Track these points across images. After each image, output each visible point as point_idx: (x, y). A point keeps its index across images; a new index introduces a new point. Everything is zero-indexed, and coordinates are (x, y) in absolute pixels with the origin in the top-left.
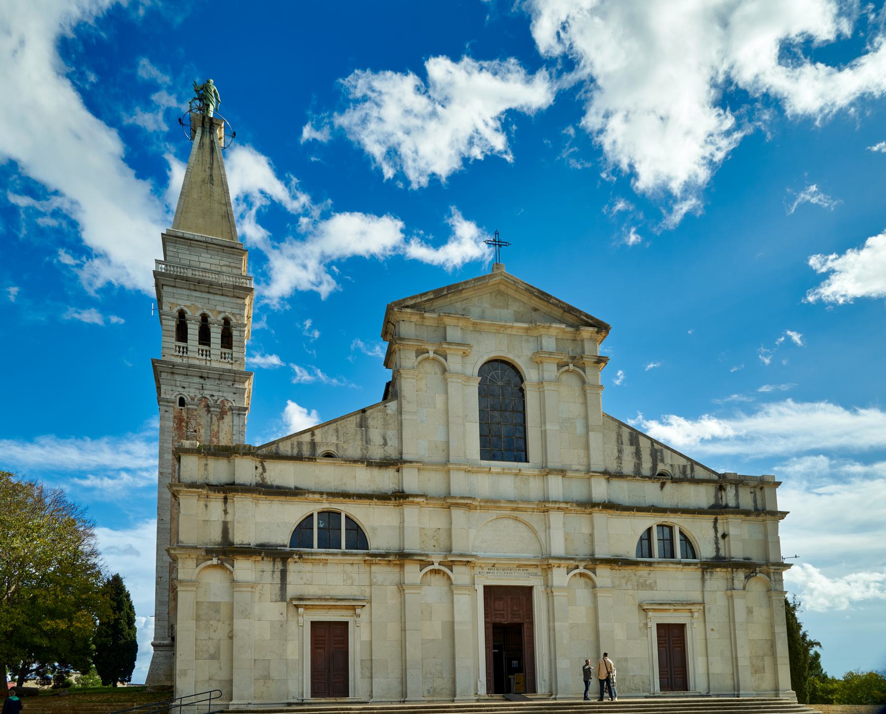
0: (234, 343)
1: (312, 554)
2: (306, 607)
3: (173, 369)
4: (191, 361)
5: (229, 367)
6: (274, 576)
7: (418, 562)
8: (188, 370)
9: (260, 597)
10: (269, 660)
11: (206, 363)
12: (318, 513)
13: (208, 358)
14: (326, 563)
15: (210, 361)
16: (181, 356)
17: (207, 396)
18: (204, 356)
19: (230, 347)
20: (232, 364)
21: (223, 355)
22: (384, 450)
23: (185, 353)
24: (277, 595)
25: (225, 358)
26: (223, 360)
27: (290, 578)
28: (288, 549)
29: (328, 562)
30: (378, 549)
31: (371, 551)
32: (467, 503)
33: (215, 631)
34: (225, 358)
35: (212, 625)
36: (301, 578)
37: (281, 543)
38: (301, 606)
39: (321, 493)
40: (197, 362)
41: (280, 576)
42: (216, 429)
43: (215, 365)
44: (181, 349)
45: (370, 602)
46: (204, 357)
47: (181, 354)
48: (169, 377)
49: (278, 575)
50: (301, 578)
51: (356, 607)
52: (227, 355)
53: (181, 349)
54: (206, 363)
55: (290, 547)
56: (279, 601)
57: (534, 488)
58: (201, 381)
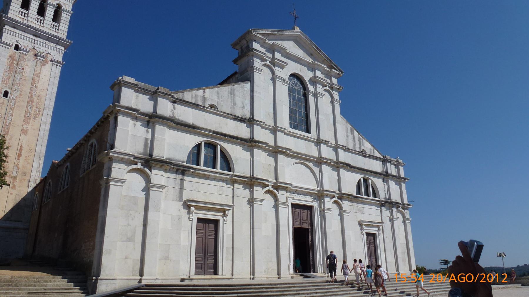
0: (62, 21)
1: (199, 170)
2: (197, 208)
3: (15, 25)
4: (29, 23)
5: (56, 34)
6: (176, 182)
7: (261, 184)
8: (26, 29)
9: (166, 197)
10: (169, 245)
11: (40, 28)
12: (205, 143)
13: (42, 24)
14: (207, 178)
15: (43, 27)
16: (22, 18)
17: (36, 48)
18: (39, 23)
19: (59, 23)
20: (58, 33)
21: (52, 26)
22: (243, 111)
23: (25, 18)
24: (177, 196)
25: (53, 28)
26: (51, 28)
27: (186, 185)
28: (186, 164)
29: (209, 177)
30: (238, 173)
31: (235, 173)
32: (287, 153)
33: (133, 219)
34: (53, 28)
35: (131, 214)
36: (193, 186)
37: (182, 160)
38: (193, 206)
39: (210, 131)
40: (34, 25)
41: (180, 183)
42: (38, 71)
43: (45, 30)
44: (23, 14)
45: (233, 207)
46: (39, 23)
47: (23, 17)
48: (11, 29)
49: (178, 181)
50: (193, 186)
51: (225, 210)
52: (55, 27)
53: (23, 14)
54: (40, 28)
55: (186, 163)
56: (178, 201)
57: (312, 150)
58: (35, 38)
